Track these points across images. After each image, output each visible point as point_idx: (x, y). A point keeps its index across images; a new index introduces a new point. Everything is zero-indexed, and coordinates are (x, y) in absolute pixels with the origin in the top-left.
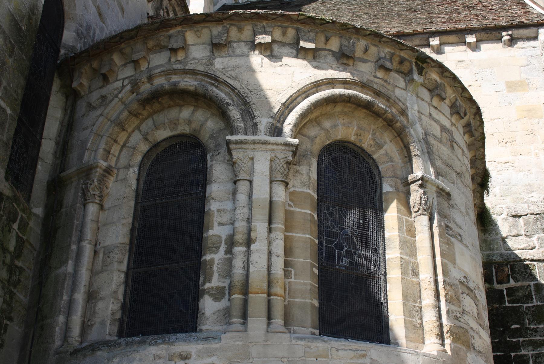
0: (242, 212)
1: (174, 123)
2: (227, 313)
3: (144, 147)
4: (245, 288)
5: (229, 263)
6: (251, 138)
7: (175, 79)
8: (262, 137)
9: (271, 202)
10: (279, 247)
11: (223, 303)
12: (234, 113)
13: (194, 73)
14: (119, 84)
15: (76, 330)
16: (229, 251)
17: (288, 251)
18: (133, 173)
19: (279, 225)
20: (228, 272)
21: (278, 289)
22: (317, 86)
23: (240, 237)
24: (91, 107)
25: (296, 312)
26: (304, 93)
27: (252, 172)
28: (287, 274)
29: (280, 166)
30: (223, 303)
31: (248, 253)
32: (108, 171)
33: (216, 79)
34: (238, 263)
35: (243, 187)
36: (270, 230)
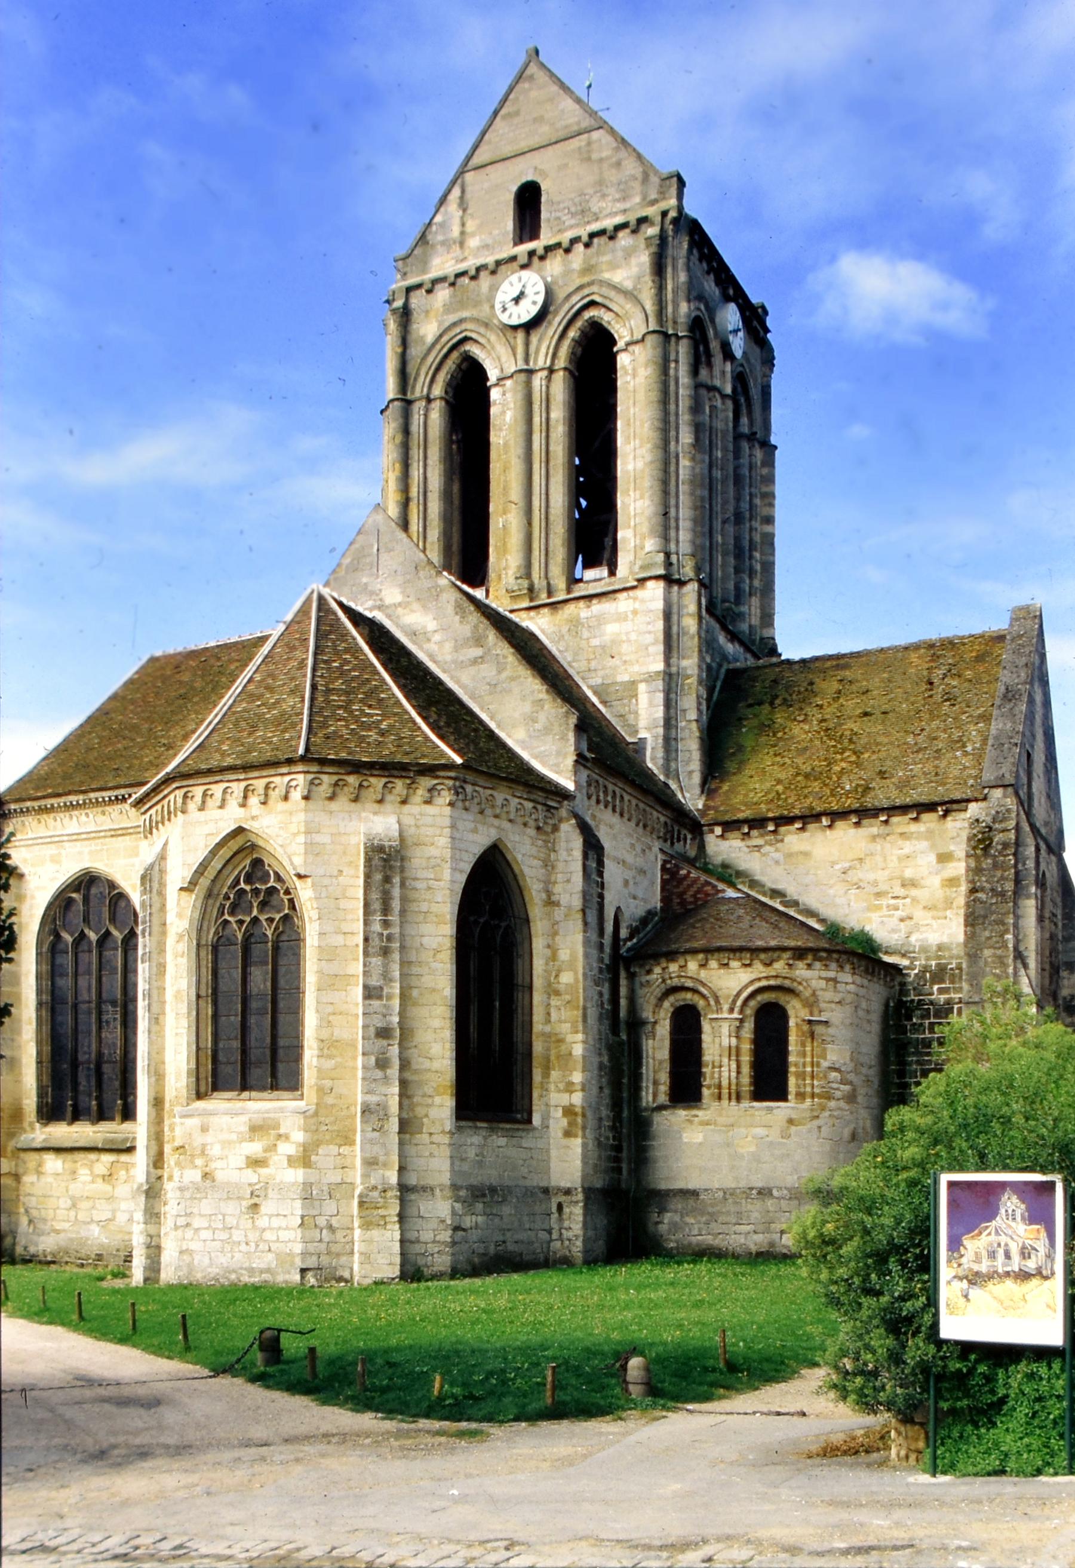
0: (717, 1052)
1: (684, 1000)
2: (713, 1094)
3: (672, 1010)
4: (719, 1087)
5: (713, 1073)
6: (720, 1016)
7: (683, 980)
8: (725, 1015)
9: (730, 1047)
10: (734, 1066)
11: (711, 1091)
12: (712, 1003)
13: (691, 978)
14: (655, 976)
15: (650, 1099)
16: (714, 1067)
17: (739, 1067)
18: (667, 1022)
19: (733, 1058)
20: (712, 1078)
21: (733, 1087)
22: (752, 982)
23: (716, 1064)
24: (642, 985)
25: (743, 1094)
26: (746, 987)
27: (720, 1032)
28: (737, 1078)
29: (733, 1028)
30: (711, 1091)
31: (720, 1072)
32: (655, 1023)
33: (704, 985)
34: (716, 1075)
35: (717, 1040)
36: (730, 1060)
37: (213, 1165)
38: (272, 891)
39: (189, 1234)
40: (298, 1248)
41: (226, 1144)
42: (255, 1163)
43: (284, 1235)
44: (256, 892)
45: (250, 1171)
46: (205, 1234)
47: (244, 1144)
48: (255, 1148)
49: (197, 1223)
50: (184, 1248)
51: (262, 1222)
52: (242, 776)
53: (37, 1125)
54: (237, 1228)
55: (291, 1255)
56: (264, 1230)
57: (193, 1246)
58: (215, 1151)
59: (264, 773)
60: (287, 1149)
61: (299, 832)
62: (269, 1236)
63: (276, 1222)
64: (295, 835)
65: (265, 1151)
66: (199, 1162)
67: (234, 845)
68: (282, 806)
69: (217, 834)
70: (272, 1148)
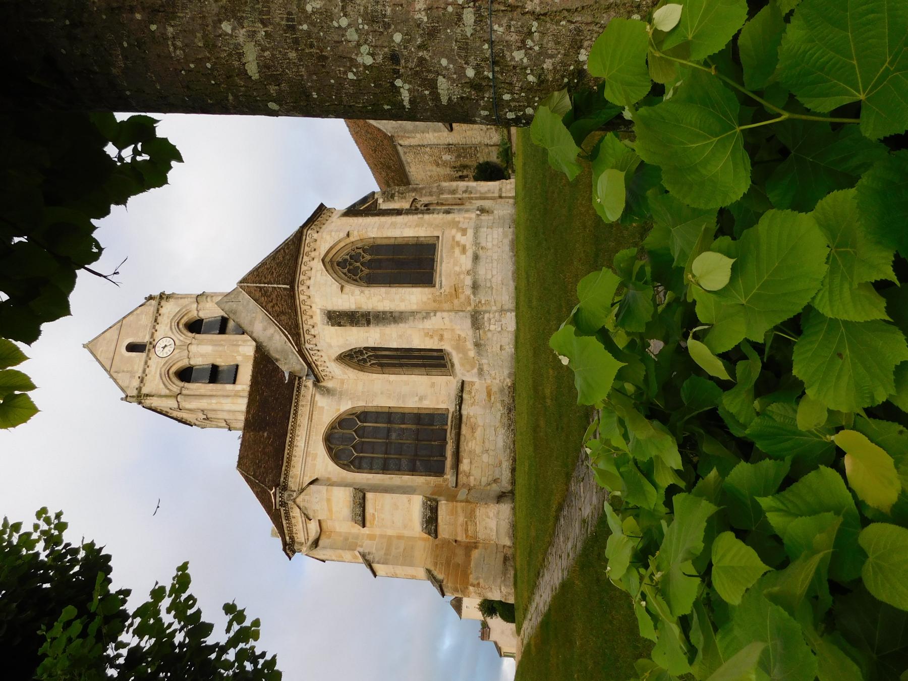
37: (464, 269)
38: (351, 257)
39: (494, 280)
40: (501, 230)
41: (455, 264)
42: (464, 250)
43: (495, 236)
44: (350, 264)
45: (467, 253)
46: (495, 272)
47: (456, 256)
48: (457, 251)
49: (489, 277)
50: (500, 282)
51: (489, 245)
52: (301, 256)
53: (445, 476)
54: (492, 257)
55: (503, 233)
56: (493, 245)
57: (500, 278)
58: (457, 269)
59: (303, 246)
60: (459, 237)
61: (331, 234)
62: (495, 242)
63: (490, 239)
64: (331, 236)
65: (459, 246)
66: (462, 276)
67: (329, 267)
68: (318, 242)
69: (322, 270)
70: (458, 243)
